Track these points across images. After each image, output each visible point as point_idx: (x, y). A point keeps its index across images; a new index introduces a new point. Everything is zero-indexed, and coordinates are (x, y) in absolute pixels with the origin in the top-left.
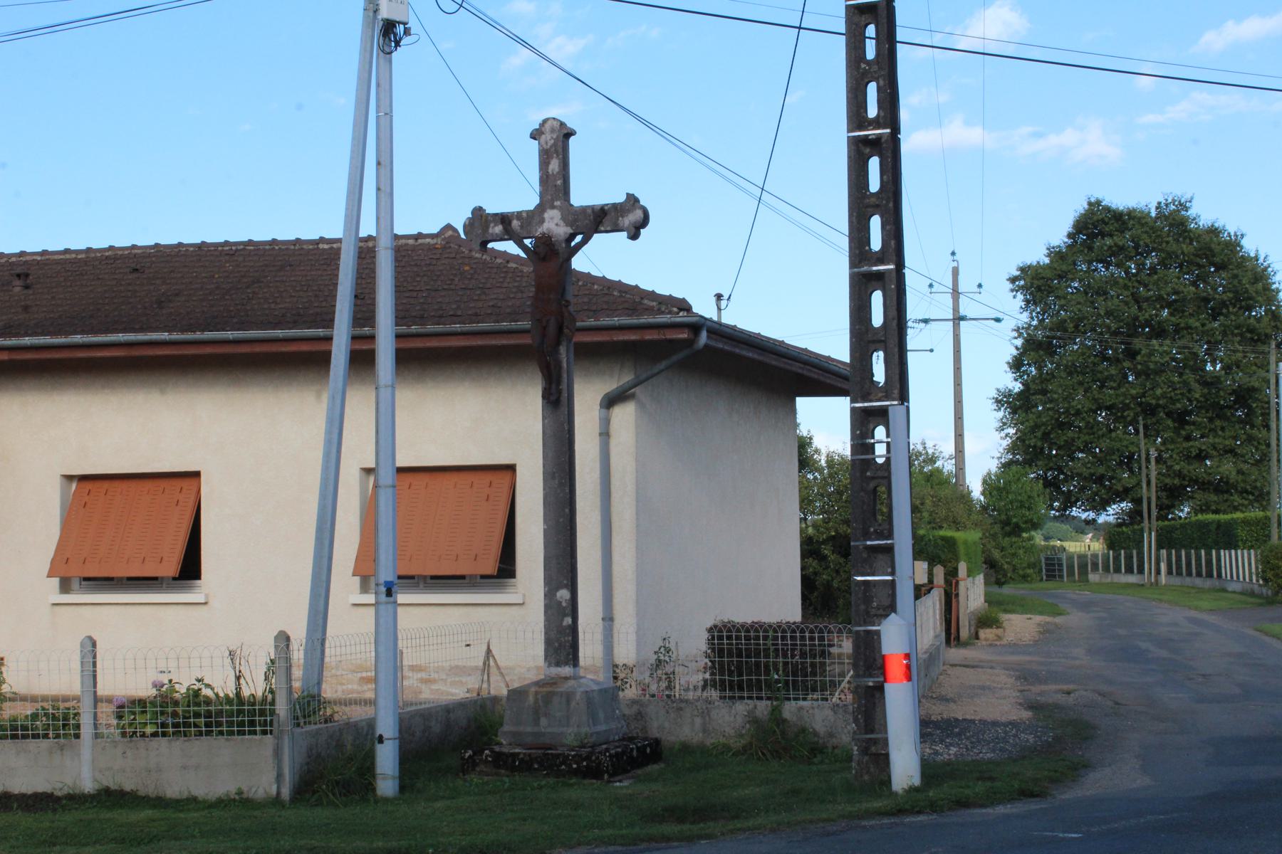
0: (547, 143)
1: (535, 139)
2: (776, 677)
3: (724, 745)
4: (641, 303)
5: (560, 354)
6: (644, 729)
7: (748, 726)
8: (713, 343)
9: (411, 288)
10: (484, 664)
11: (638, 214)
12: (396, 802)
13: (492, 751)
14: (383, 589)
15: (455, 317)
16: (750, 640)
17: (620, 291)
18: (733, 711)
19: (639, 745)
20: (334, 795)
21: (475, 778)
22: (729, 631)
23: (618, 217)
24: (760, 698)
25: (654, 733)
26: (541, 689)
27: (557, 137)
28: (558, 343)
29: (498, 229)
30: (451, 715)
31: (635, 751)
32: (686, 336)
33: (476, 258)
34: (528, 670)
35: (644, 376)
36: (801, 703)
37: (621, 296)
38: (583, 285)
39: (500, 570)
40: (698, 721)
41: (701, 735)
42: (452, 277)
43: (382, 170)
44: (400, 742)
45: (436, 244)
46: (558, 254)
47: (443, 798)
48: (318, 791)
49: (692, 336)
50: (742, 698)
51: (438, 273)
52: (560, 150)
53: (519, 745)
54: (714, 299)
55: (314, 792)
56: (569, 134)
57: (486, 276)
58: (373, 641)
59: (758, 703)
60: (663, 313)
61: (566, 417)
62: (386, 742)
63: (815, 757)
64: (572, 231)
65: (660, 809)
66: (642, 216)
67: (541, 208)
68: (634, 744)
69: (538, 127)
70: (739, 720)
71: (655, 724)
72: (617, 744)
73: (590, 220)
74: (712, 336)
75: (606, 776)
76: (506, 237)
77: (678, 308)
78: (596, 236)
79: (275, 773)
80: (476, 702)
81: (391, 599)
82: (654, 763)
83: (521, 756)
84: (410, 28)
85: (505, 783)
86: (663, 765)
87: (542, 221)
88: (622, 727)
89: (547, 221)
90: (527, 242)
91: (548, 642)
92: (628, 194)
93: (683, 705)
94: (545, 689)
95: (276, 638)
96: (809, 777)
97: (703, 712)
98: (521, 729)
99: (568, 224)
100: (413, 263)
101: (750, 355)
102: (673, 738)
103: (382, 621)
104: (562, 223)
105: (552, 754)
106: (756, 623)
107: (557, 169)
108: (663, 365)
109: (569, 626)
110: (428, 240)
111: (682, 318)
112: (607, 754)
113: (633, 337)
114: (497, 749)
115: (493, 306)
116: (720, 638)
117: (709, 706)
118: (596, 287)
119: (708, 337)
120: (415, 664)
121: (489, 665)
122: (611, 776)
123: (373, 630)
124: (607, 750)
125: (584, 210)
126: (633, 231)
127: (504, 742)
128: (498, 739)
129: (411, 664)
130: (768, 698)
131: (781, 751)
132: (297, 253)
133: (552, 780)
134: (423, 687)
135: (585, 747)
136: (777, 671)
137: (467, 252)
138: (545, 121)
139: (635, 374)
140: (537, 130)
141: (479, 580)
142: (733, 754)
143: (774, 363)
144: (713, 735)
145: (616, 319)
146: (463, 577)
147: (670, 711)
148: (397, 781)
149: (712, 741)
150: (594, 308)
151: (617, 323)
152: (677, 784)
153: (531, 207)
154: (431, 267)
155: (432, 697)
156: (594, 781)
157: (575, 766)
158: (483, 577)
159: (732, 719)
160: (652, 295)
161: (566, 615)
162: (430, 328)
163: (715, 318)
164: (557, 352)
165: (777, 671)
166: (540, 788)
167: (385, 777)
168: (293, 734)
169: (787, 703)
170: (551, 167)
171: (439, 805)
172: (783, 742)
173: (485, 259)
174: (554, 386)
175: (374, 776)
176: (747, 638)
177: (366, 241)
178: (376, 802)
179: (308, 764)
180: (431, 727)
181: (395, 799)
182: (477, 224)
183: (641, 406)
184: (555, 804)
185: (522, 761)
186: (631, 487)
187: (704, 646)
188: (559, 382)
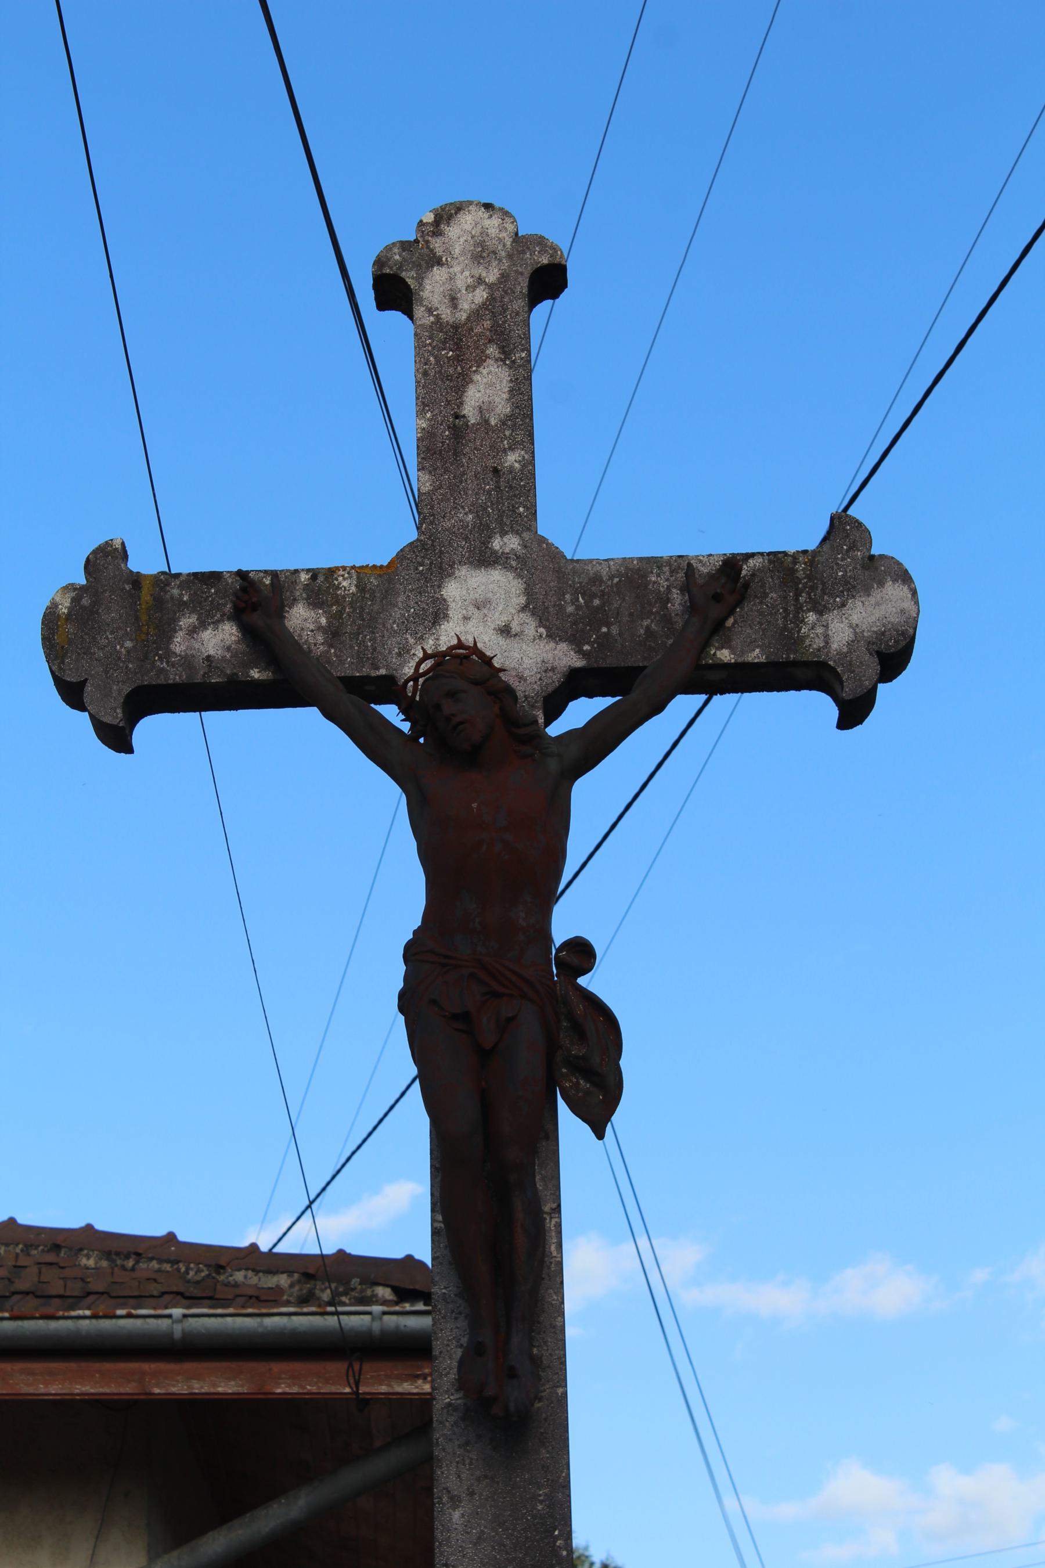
0: (454, 301)
23: (799, 608)
27: (504, 277)
64: (579, 663)
77: (395, 1289)
87: (438, 614)
89: (455, 612)
104: (531, 627)
138: (445, 216)
140: (405, 246)
145: (177, 1312)
151: (178, 1330)
153: (383, 558)
170: (474, 398)
182: (112, 614)
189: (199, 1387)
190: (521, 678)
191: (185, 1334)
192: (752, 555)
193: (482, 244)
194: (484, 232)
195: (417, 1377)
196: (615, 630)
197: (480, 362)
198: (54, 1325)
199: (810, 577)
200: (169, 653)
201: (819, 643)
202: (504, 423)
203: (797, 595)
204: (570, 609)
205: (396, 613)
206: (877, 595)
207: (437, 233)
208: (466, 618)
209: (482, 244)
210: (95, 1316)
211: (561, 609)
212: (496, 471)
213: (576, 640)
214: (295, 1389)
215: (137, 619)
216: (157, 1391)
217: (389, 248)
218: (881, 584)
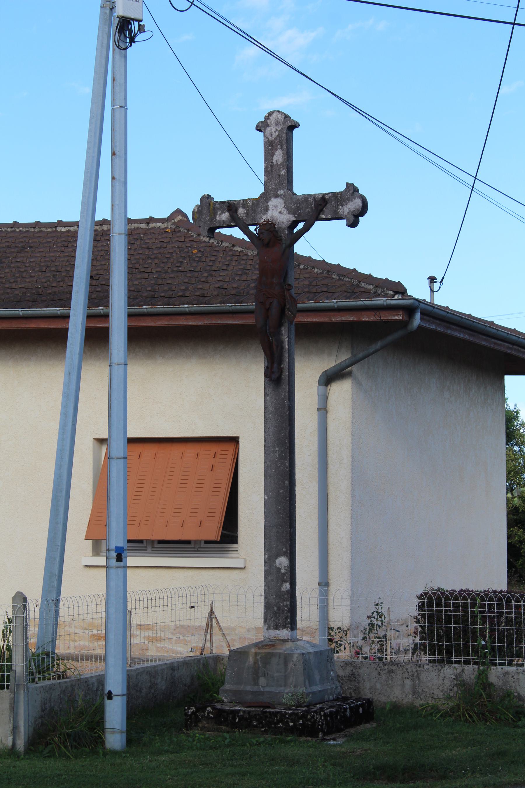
0: (271, 135)
1: (260, 131)
2: (483, 643)
3: (433, 707)
4: (358, 286)
5: (282, 335)
6: (357, 690)
7: (455, 688)
8: (426, 325)
9: (142, 270)
10: (207, 625)
11: (357, 204)
12: (124, 755)
13: (214, 708)
14: (114, 555)
15: (183, 298)
16: (458, 607)
17: (339, 275)
18: (442, 674)
19: (352, 705)
20: (66, 747)
21: (197, 733)
22: (439, 598)
23: (338, 205)
24: (467, 663)
25: (367, 694)
26: (260, 651)
27: (282, 129)
28: (280, 325)
29: (225, 216)
30: (176, 672)
31: (348, 710)
32: (401, 318)
33: (204, 242)
34: (249, 630)
35: (360, 355)
36: (507, 668)
37: (340, 279)
38: (304, 269)
39: (223, 535)
40: (408, 682)
41: (411, 696)
42: (181, 260)
43: (117, 160)
44: (128, 698)
45: (167, 228)
46: (281, 240)
47: (167, 752)
48: (51, 744)
49: (406, 318)
50: (451, 662)
51: (168, 256)
52: (284, 142)
53: (239, 703)
54: (428, 282)
55: (47, 744)
56: (293, 126)
57: (213, 259)
58: (104, 602)
59: (466, 667)
60: (379, 296)
61: (287, 394)
62: (114, 698)
63: (520, 720)
64: (295, 219)
65: (372, 767)
66: (361, 204)
67: (265, 197)
68: (348, 704)
69: (263, 120)
70: (447, 683)
71: (368, 685)
72: (331, 704)
73: (312, 208)
74: (425, 317)
75: (321, 735)
76: (232, 224)
77: (394, 291)
78: (317, 223)
79: (11, 725)
80: (199, 660)
81: (121, 564)
82: (366, 723)
83: (242, 713)
84: (144, 25)
85: (226, 739)
86: (374, 725)
87: (267, 209)
88: (337, 687)
89: (271, 209)
90: (252, 228)
91: (268, 606)
92: (347, 184)
93: (394, 668)
94: (264, 651)
95: (14, 599)
96: (514, 740)
97: (413, 675)
98: (242, 687)
99: (291, 211)
100: (144, 246)
101: (461, 336)
102: (383, 699)
103: (112, 584)
104: (285, 211)
105: (270, 712)
106: (465, 591)
107: (281, 160)
108: (379, 344)
109: (287, 591)
110: (159, 224)
111: (397, 300)
112: (322, 713)
113: (350, 318)
114: (218, 706)
115: (218, 287)
116: (430, 605)
117: (419, 669)
118: (316, 270)
119: (422, 319)
120: (142, 623)
121: (212, 625)
122: (325, 734)
123: (103, 591)
124: (322, 709)
125: (306, 198)
126: (352, 219)
127: (225, 700)
128: (220, 696)
129: (138, 623)
130: (475, 663)
131: (487, 714)
132: (37, 235)
133: (269, 737)
134: (150, 644)
135: (301, 707)
136: (484, 637)
137: (195, 236)
138: (270, 114)
139: (352, 354)
140: (262, 122)
141: (203, 545)
142: (441, 716)
143: (484, 343)
144: (422, 697)
146: (188, 542)
147: (381, 672)
148: (124, 735)
149: (421, 702)
150: (314, 290)
151: (336, 305)
152: (388, 743)
154: (162, 250)
155: (159, 654)
156: (310, 739)
157: (291, 724)
158: (207, 542)
159: (441, 682)
160: (369, 278)
161: (285, 581)
162: (160, 308)
163: (428, 300)
164: (279, 333)
165: (484, 637)
166: (259, 744)
167: (114, 731)
168: (28, 689)
169: (493, 667)
170: (275, 158)
171: (163, 758)
172: (489, 705)
173: (213, 243)
174: (275, 365)
175: (103, 730)
176: (456, 606)
177: (101, 225)
178: (105, 755)
179: (41, 717)
180: (157, 684)
181: (123, 752)
183: (358, 384)
184: (273, 760)
185: (241, 718)
186: (347, 460)
187: (414, 612)
188: (280, 362)
189: (344, 319)
190: (283, 223)
191: (338, 306)
192: (329, 193)
193: (277, 121)
194: (278, 118)
195: (399, 315)
196: (302, 211)
197: (276, 150)
198: (305, 305)
199: (340, 198)
200: (216, 220)
201: (342, 213)
202: (281, 164)
203: (338, 202)
204: (293, 207)
205: (259, 209)
206: (354, 201)
207: (268, 119)
208: (273, 210)
209: (277, 121)
210: (315, 303)
211: (291, 207)
212: (279, 175)
213: (294, 214)
214: (368, 319)
215: (210, 212)
216: (333, 320)
217: (259, 123)
218: (355, 199)
